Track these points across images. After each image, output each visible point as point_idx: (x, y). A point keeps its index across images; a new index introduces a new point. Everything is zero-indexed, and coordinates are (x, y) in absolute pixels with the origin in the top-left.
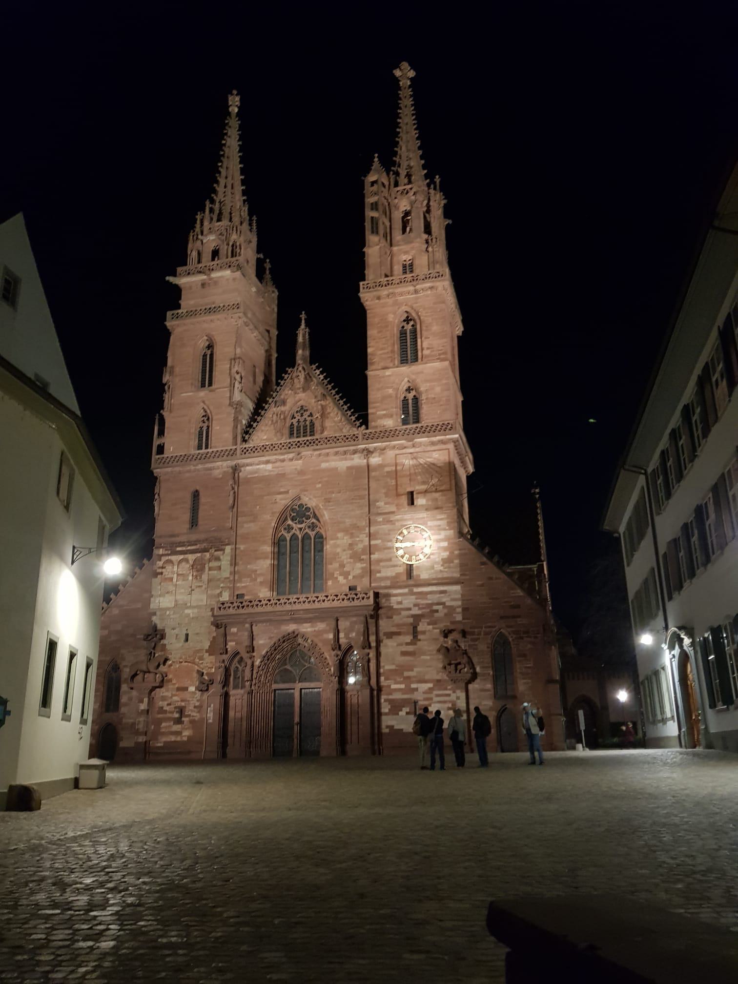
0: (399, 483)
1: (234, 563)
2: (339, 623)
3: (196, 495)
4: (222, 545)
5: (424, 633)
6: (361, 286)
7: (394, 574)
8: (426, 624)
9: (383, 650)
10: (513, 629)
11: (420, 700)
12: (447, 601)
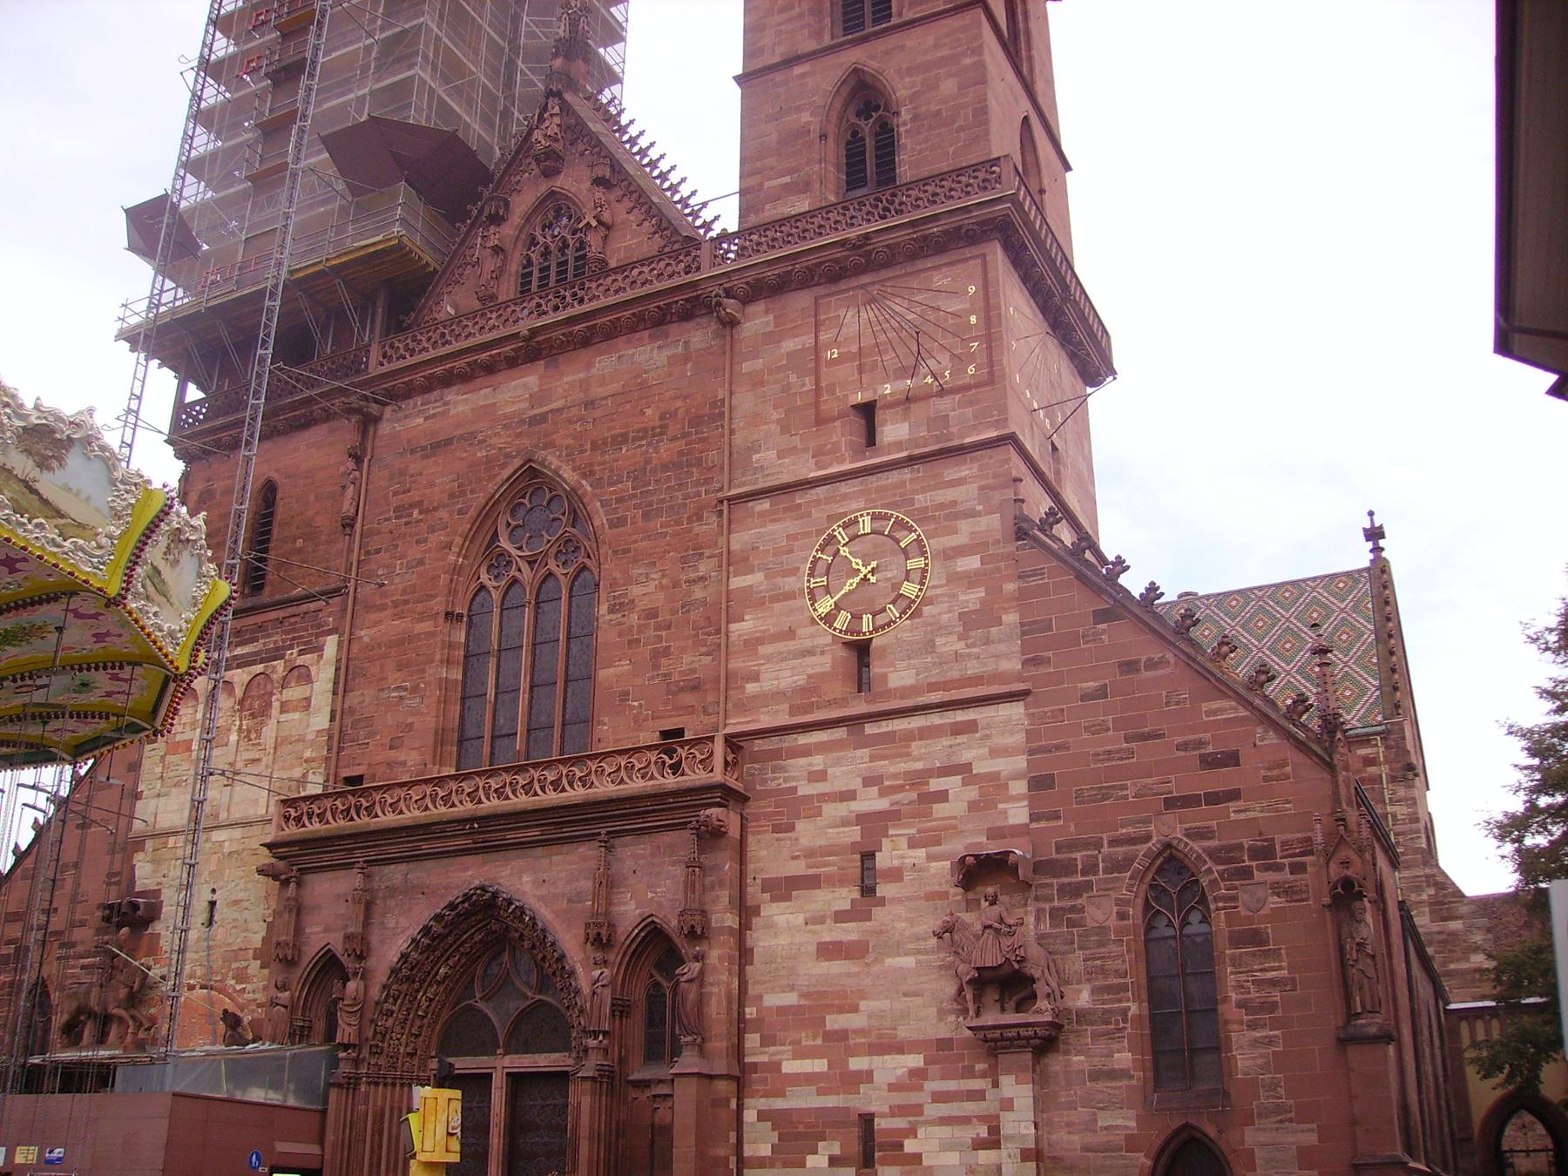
1: (343, 683)
4: (317, 636)
5: (895, 875)
7: (801, 680)
8: (904, 843)
9: (761, 941)
10: (1214, 843)
11: (883, 1115)
12: (980, 758)
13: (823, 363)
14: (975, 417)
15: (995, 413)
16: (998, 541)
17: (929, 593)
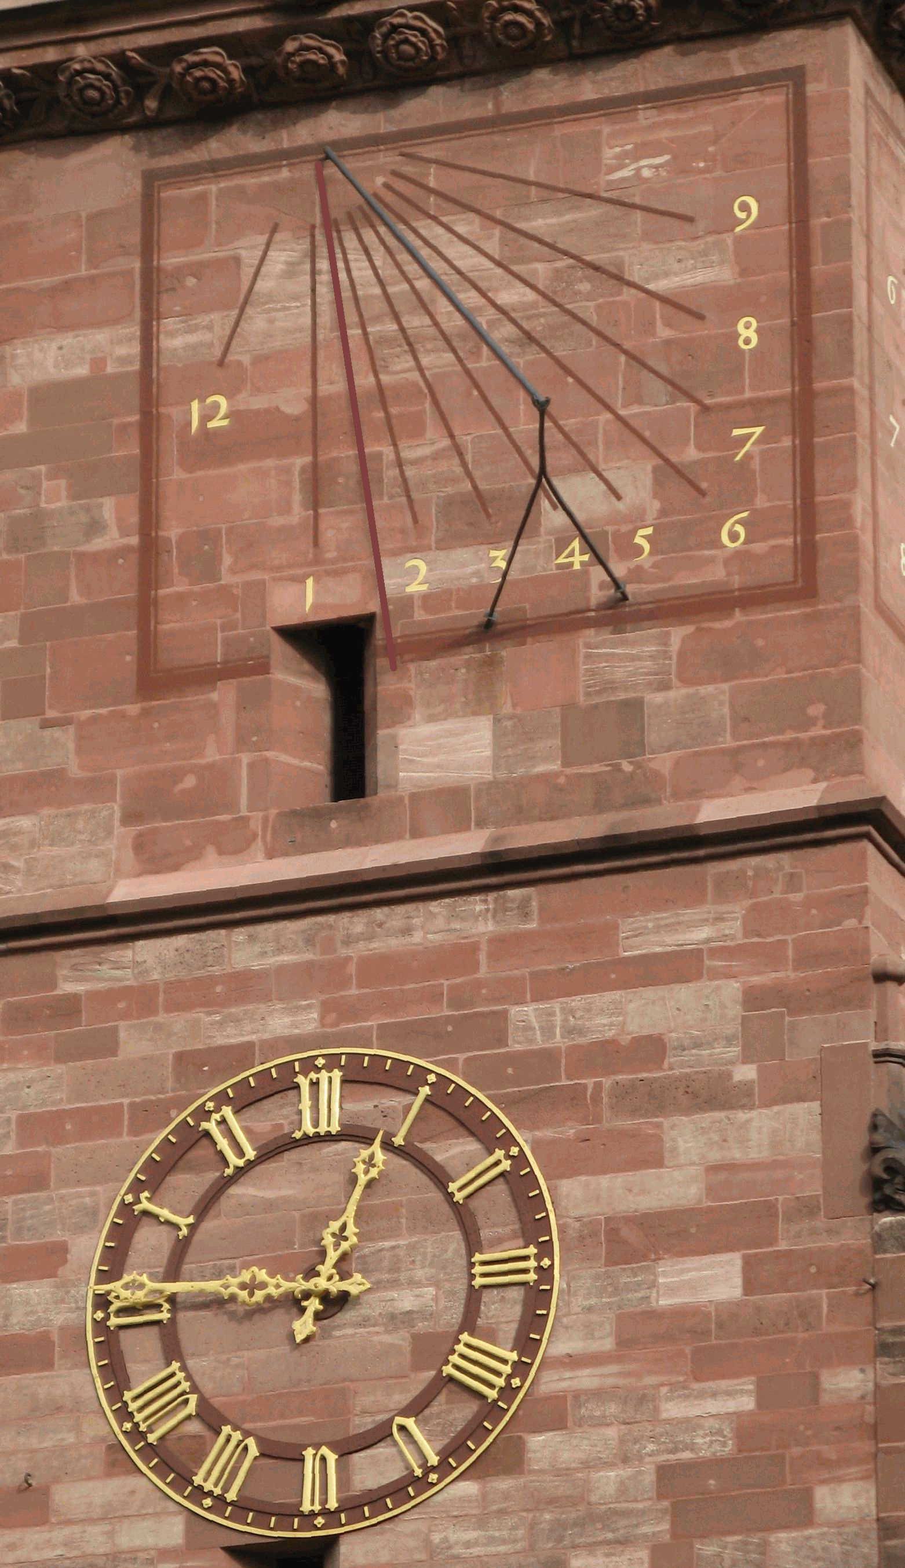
0: (172, 531)
13: (170, 448)
14: (741, 720)
15: (816, 710)
16: (807, 1209)
17: (553, 1383)
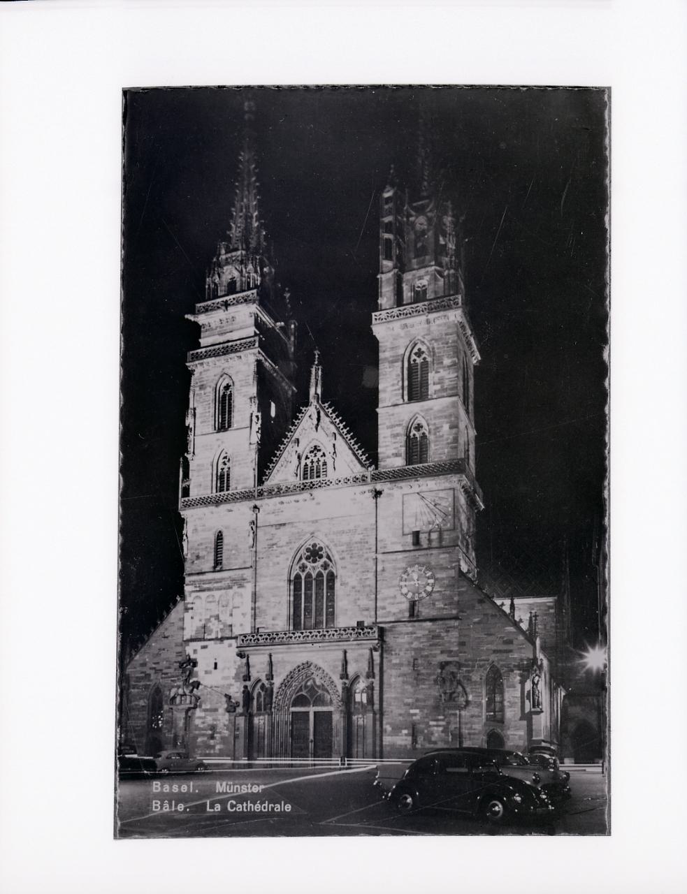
2: (348, 655)
3: (220, 537)
6: (374, 317)
